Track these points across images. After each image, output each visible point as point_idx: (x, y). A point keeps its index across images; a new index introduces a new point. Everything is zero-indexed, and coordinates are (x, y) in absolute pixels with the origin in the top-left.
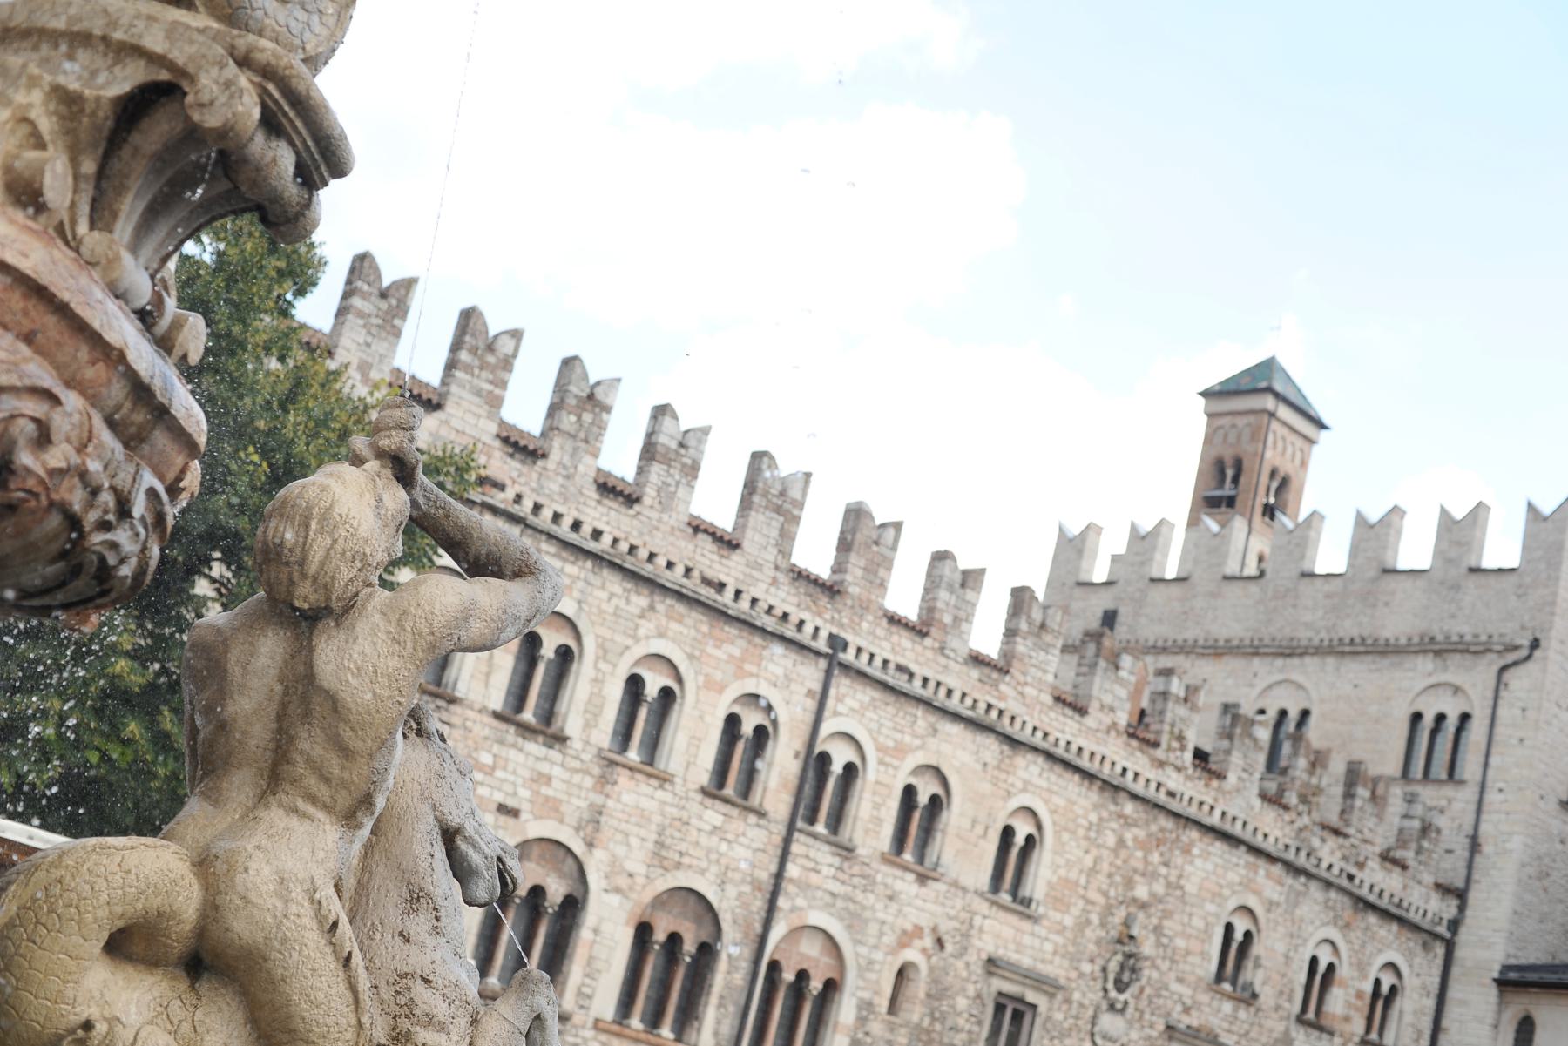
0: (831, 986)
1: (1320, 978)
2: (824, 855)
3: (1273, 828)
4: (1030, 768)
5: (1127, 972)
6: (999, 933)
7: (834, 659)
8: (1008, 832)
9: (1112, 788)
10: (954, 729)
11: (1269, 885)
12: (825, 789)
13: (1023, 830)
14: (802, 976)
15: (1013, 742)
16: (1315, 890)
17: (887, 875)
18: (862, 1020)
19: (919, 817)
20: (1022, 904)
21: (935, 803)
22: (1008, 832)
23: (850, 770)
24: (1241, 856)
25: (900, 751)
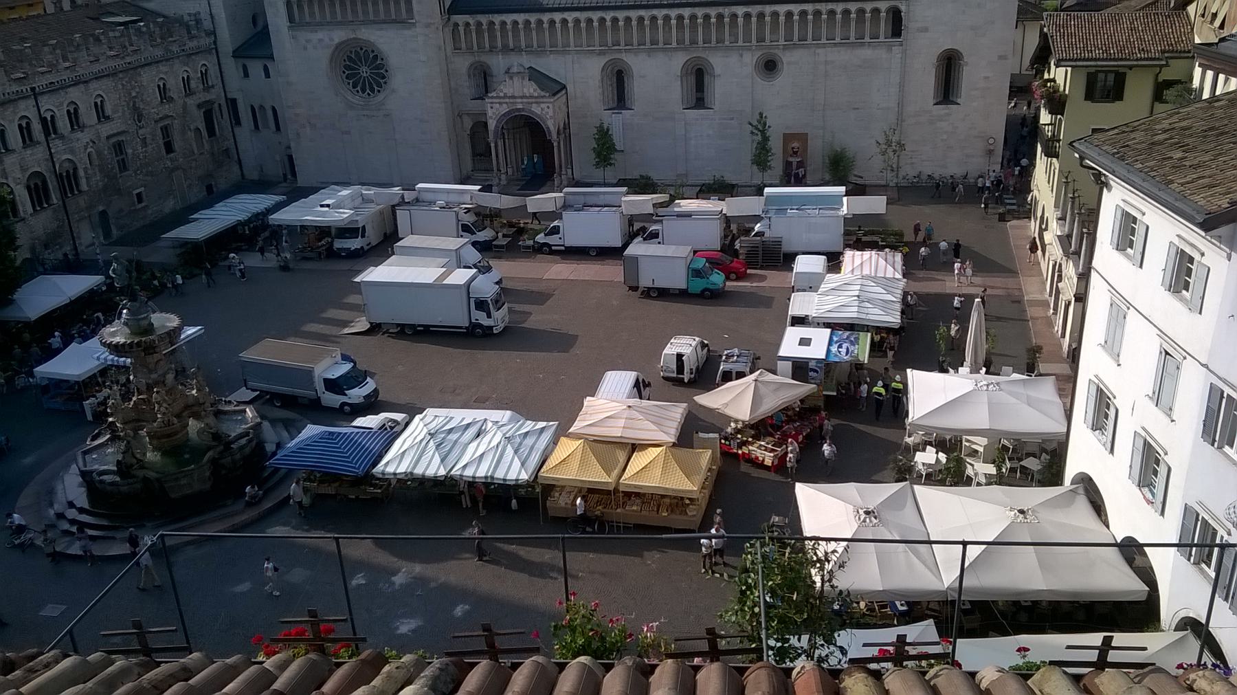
0: (75, 169)
1: (186, 82)
2: (58, 142)
3: (158, 52)
4: (93, 85)
5: (140, 117)
6: (106, 129)
7: (35, 94)
8: (96, 104)
9: (113, 74)
10: (71, 89)
11: (163, 68)
12: (49, 126)
13: (99, 100)
14: (68, 172)
15: (86, 82)
16: (176, 61)
17: (74, 136)
18: (86, 173)
19: (74, 116)
20: (107, 118)
21: (76, 110)
22: (96, 104)
23: (52, 117)
24: (154, 67)
25: (61, 104)
